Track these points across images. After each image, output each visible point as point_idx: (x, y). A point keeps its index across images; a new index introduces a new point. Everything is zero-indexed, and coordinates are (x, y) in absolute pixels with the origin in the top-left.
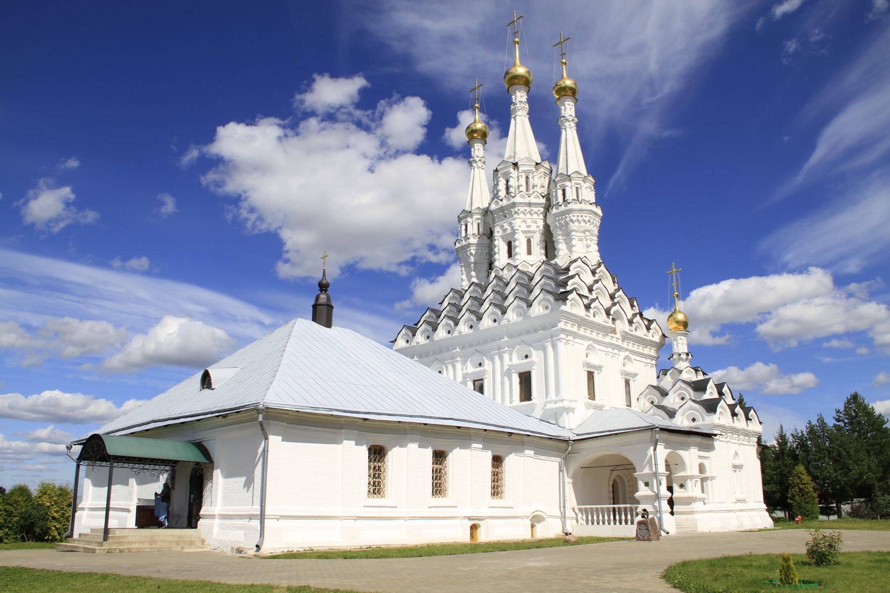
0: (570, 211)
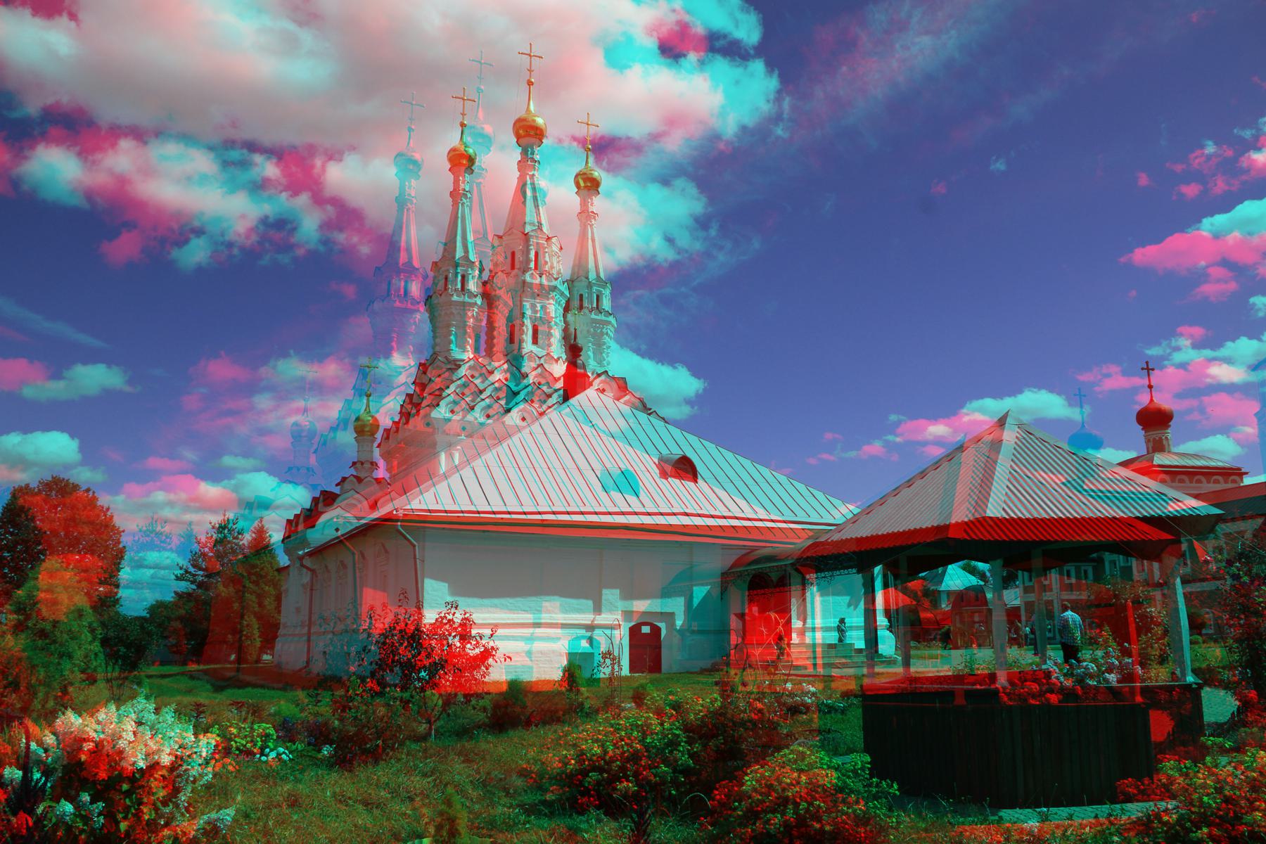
0: (609, 323)
